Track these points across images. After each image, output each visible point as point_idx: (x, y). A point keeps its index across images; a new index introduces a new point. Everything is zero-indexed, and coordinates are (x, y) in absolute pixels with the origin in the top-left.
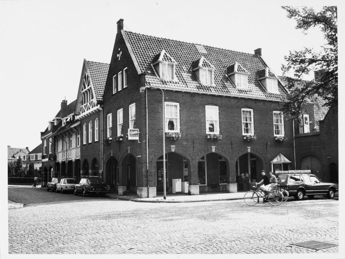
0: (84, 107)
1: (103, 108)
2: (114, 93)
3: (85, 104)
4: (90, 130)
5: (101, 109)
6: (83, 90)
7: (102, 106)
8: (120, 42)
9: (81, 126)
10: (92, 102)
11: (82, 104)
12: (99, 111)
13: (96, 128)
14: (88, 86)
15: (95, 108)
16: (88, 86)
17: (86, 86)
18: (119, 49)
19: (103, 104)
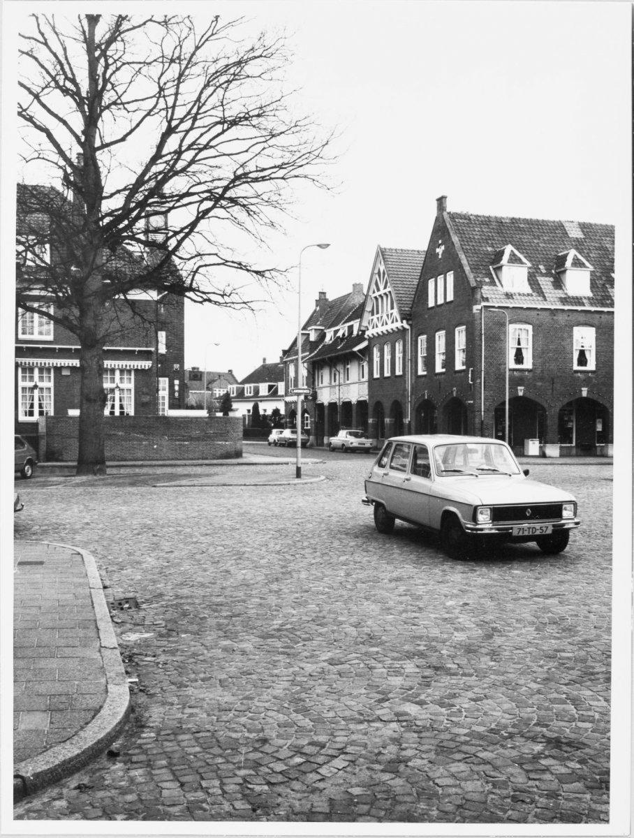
0: (375, 320)
3: (379, 315)
4: (387, 357)
5: (407, 327)
6: (374, 292)
7: (410, 322)
8: (439, 232)
10: (392, 314)
11: (373, 315)
12: (405, 329)
13: (399, 355)
14: (385, 288)
15: (399, 324)
16: (385, 288)
17: (381, 287)
18: (440, 242)
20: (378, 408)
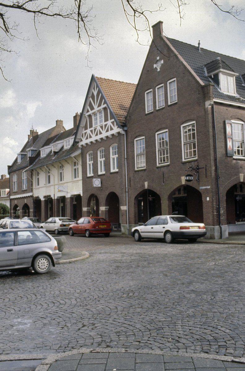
1: (126, 131)
2: (147, 113)
3: (93, 129)
5: (123, 132)
6: (88, 111)
7: (126, 129)
9: (83, 155)
11: (86, 129)
18: (158, 58)
19: (126, 126)
20: (93, 198)
